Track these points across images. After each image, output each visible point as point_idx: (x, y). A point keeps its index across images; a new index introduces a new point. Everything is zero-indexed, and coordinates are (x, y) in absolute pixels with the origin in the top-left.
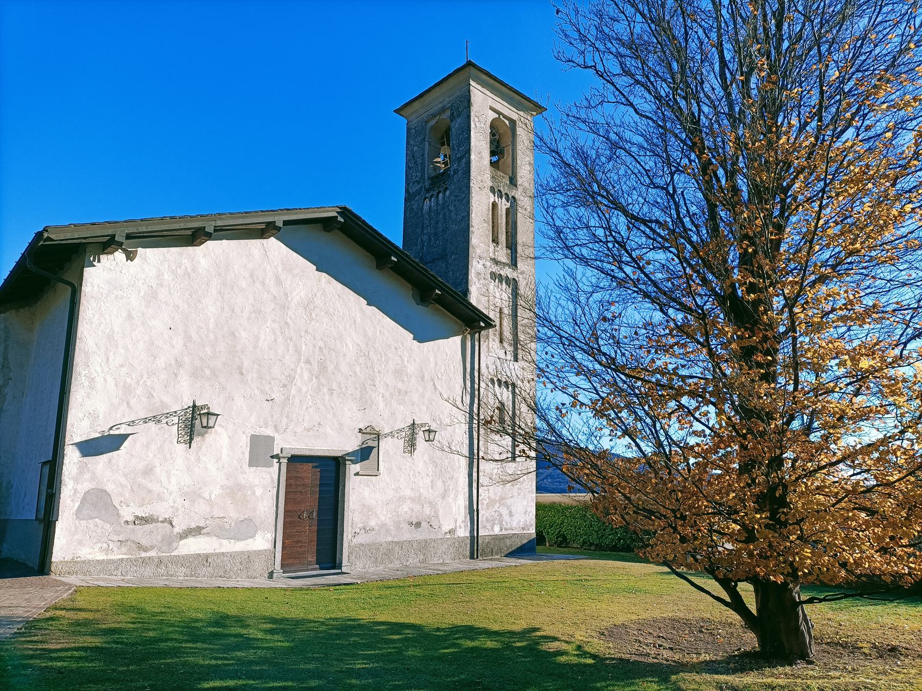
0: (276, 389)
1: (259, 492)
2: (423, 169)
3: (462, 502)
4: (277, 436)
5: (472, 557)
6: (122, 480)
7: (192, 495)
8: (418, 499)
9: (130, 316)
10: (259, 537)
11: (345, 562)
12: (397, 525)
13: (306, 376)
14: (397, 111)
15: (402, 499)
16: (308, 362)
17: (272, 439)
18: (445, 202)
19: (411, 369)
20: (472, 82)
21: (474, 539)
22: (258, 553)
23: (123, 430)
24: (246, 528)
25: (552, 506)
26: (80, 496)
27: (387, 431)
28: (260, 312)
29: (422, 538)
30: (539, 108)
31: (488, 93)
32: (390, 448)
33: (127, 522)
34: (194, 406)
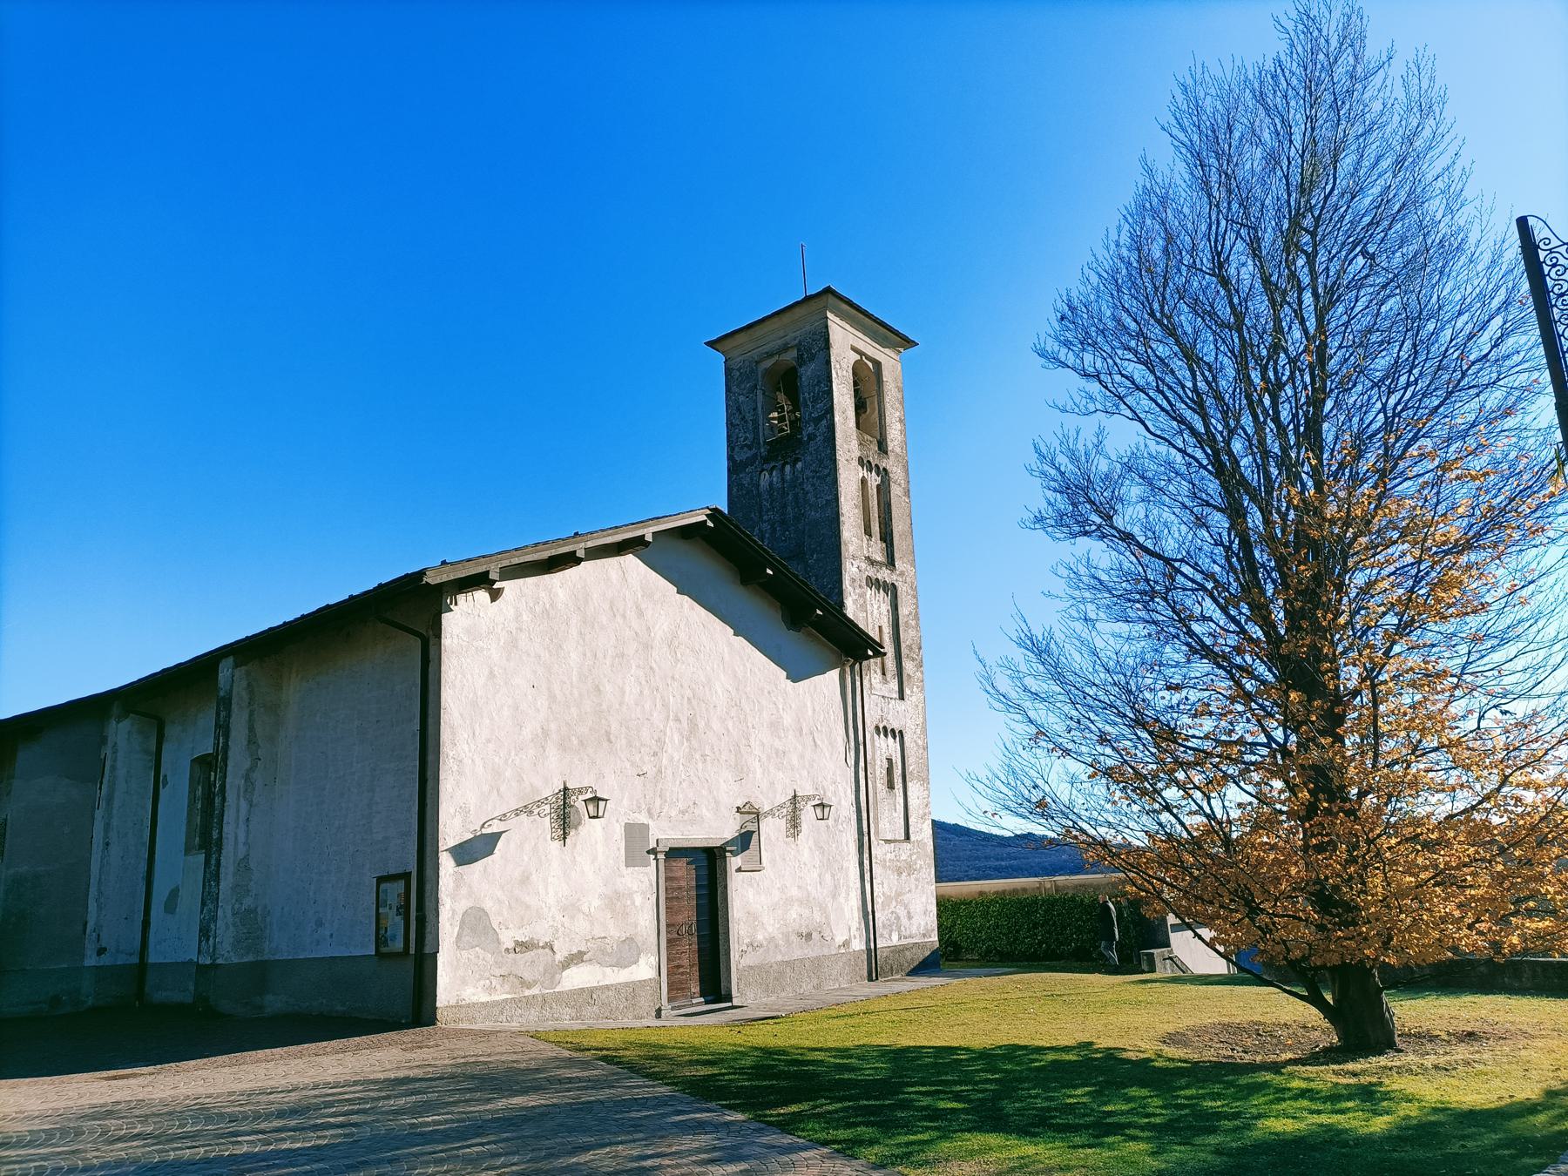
0: (647, 758)
1: (638, 900)
2: (756, 428)
3: (854, 901)
4: (651, 824)
5: (870, 979)
6: (499, 893)
7: (571, 908)
8: (806, 901)
9: (492, 675)
10: (642, 961)
11: (734, 993)
12: (786, 936)
13: (676, 738)
14: (708, 344)
15: (789, 901)
16: (678, 720)
17: (647, 827)
18: (795, 478)
19: (788, 720)
20: (829, 315)
21: (871, 953)
22: (643, 983)
23: (495, 828)
24: (626, 953)
25: (983, 904)
26: (458, 917)
27: (766, 808)
28: (623, 655)
29: (812, 954)
30: (908, 343)
31: (848, 327)
32: (771, 830)
33: (507, 950)
34: (566, 789)
